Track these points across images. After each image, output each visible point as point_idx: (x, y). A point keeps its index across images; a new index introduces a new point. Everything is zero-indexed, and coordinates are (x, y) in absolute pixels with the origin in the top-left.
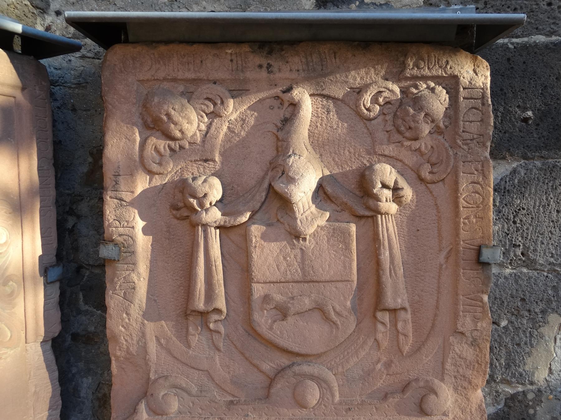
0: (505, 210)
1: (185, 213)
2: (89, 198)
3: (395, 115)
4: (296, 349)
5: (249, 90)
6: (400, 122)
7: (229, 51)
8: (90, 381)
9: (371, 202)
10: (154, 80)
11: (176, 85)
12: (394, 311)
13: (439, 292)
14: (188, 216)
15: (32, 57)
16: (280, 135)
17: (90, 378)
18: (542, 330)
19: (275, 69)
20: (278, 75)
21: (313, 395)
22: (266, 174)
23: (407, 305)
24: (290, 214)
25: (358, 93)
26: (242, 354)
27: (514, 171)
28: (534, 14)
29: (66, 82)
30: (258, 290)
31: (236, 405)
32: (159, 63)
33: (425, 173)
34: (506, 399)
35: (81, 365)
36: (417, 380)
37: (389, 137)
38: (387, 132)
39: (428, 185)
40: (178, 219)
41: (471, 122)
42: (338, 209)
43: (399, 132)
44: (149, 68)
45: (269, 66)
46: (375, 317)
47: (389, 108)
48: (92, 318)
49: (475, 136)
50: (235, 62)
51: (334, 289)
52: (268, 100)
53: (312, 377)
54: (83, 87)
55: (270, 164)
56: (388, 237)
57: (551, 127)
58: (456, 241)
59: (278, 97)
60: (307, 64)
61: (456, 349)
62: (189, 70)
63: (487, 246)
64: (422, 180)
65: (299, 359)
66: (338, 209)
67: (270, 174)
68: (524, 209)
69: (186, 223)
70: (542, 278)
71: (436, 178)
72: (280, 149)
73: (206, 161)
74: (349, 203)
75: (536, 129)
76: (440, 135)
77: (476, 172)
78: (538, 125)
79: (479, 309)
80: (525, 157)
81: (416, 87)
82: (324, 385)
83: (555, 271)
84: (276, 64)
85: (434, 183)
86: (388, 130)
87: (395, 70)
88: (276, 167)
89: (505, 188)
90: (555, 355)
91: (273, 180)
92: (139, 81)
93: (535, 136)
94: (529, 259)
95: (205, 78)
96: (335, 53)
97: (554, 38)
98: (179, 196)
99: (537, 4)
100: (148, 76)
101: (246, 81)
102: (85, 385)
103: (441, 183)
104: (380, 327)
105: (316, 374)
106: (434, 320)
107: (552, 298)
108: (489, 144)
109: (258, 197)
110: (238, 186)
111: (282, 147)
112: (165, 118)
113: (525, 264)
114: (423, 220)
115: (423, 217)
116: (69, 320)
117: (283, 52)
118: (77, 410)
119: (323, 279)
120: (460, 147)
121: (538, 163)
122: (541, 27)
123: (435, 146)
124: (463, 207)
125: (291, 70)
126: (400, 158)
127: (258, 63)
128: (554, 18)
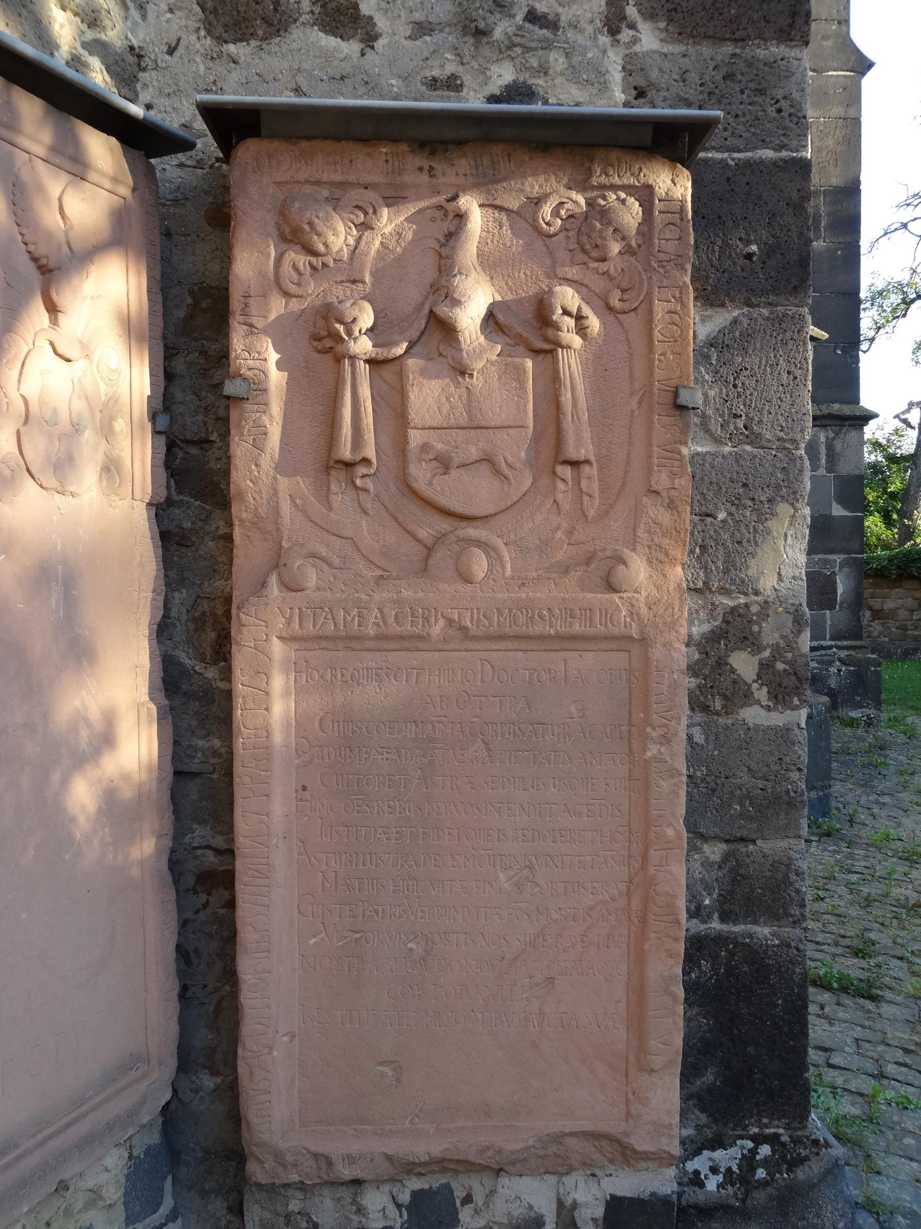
0: (724, 370)
1: (328, 343)
2: (186, 352)
3: (579, 231)
4: (459, 508)
6: (584, 239)
7: (384, 150)
8: (184, 595)
9: (550, 332)
10: (294, 182)
11: (320, 189)
13: (630, 444)
14: (332, 348)
15: (143, 153)
16: (444, 251)
17: (184, 591)
18: (769, 524)
19: (438, 173)
20: (442, 180)
21: (480, 565)
22: (427, 298)
23: (593, 459)
25: (536, 204)
26: (394, 518)
27: (735, 321)
28: (760, 122)
30: (416, 438)
32: (300, 162)
33: (615, 302)
34: (724, 614)
36: (604, 550)
37: (573, 257)
38: (570, 251)
40: (319, 352)
41: (668, 240)
42: (512, 342)
43: (584, 251)
45: (431, 169)
46: (554, 472)
48: (188, 511)
49: (673, 257)
50: (390, 162)
51: (506, 437)
52: (429, 211)
54: (181, 205)
55: (431, 287)
56: (570, 376)
57: (781, 265)
60: (477, 167)
61: (650, 511)
62: (336, 171)
63: (685, 387)
64: (610, 309)
65: (463, 524)
66: (512, 342)
67: (431, 298)
68: (746, 369)
69: (328, 358)
70: (770, 458)
71: (626, 306)
72: (443, 268)
73: (354, 282)
74: (525, 334)
77: (673, 300)
78: (764, 263)
79: (677, 463)
80: (749, 304)
81: (604, 198)
82: (493, 554)
83: (786, 448)
84: (439, 167)
85: (624, 312)
86: (571, 248)
87: (580, 178)
88: (438, 290)
89: (723, 342)
91: (435, 305)
92: (275, 183)
93: (761, 276)
95: (355, 181)
97: (785, 154)
98: (321, 323)
99: (764, 111)
100: (286, 177)
101: (403, 186)
102: (178, 601)
103: (633, 313)
104: (560, 484)
105: (484, 539)
106: (624, 478)
108: (689, 267)
109: (416, 325)
110: (393, 313)
111: (445, 265)
112: (307, 227)
114: (613, 358)
117: (448, 154)
119: (492, 424)
120: (655, 269)
121: (765, 312)
122: (768, 139)
123: (626, 269)
126: (585, 282)
127: (418, 165)
128: (784, 128)
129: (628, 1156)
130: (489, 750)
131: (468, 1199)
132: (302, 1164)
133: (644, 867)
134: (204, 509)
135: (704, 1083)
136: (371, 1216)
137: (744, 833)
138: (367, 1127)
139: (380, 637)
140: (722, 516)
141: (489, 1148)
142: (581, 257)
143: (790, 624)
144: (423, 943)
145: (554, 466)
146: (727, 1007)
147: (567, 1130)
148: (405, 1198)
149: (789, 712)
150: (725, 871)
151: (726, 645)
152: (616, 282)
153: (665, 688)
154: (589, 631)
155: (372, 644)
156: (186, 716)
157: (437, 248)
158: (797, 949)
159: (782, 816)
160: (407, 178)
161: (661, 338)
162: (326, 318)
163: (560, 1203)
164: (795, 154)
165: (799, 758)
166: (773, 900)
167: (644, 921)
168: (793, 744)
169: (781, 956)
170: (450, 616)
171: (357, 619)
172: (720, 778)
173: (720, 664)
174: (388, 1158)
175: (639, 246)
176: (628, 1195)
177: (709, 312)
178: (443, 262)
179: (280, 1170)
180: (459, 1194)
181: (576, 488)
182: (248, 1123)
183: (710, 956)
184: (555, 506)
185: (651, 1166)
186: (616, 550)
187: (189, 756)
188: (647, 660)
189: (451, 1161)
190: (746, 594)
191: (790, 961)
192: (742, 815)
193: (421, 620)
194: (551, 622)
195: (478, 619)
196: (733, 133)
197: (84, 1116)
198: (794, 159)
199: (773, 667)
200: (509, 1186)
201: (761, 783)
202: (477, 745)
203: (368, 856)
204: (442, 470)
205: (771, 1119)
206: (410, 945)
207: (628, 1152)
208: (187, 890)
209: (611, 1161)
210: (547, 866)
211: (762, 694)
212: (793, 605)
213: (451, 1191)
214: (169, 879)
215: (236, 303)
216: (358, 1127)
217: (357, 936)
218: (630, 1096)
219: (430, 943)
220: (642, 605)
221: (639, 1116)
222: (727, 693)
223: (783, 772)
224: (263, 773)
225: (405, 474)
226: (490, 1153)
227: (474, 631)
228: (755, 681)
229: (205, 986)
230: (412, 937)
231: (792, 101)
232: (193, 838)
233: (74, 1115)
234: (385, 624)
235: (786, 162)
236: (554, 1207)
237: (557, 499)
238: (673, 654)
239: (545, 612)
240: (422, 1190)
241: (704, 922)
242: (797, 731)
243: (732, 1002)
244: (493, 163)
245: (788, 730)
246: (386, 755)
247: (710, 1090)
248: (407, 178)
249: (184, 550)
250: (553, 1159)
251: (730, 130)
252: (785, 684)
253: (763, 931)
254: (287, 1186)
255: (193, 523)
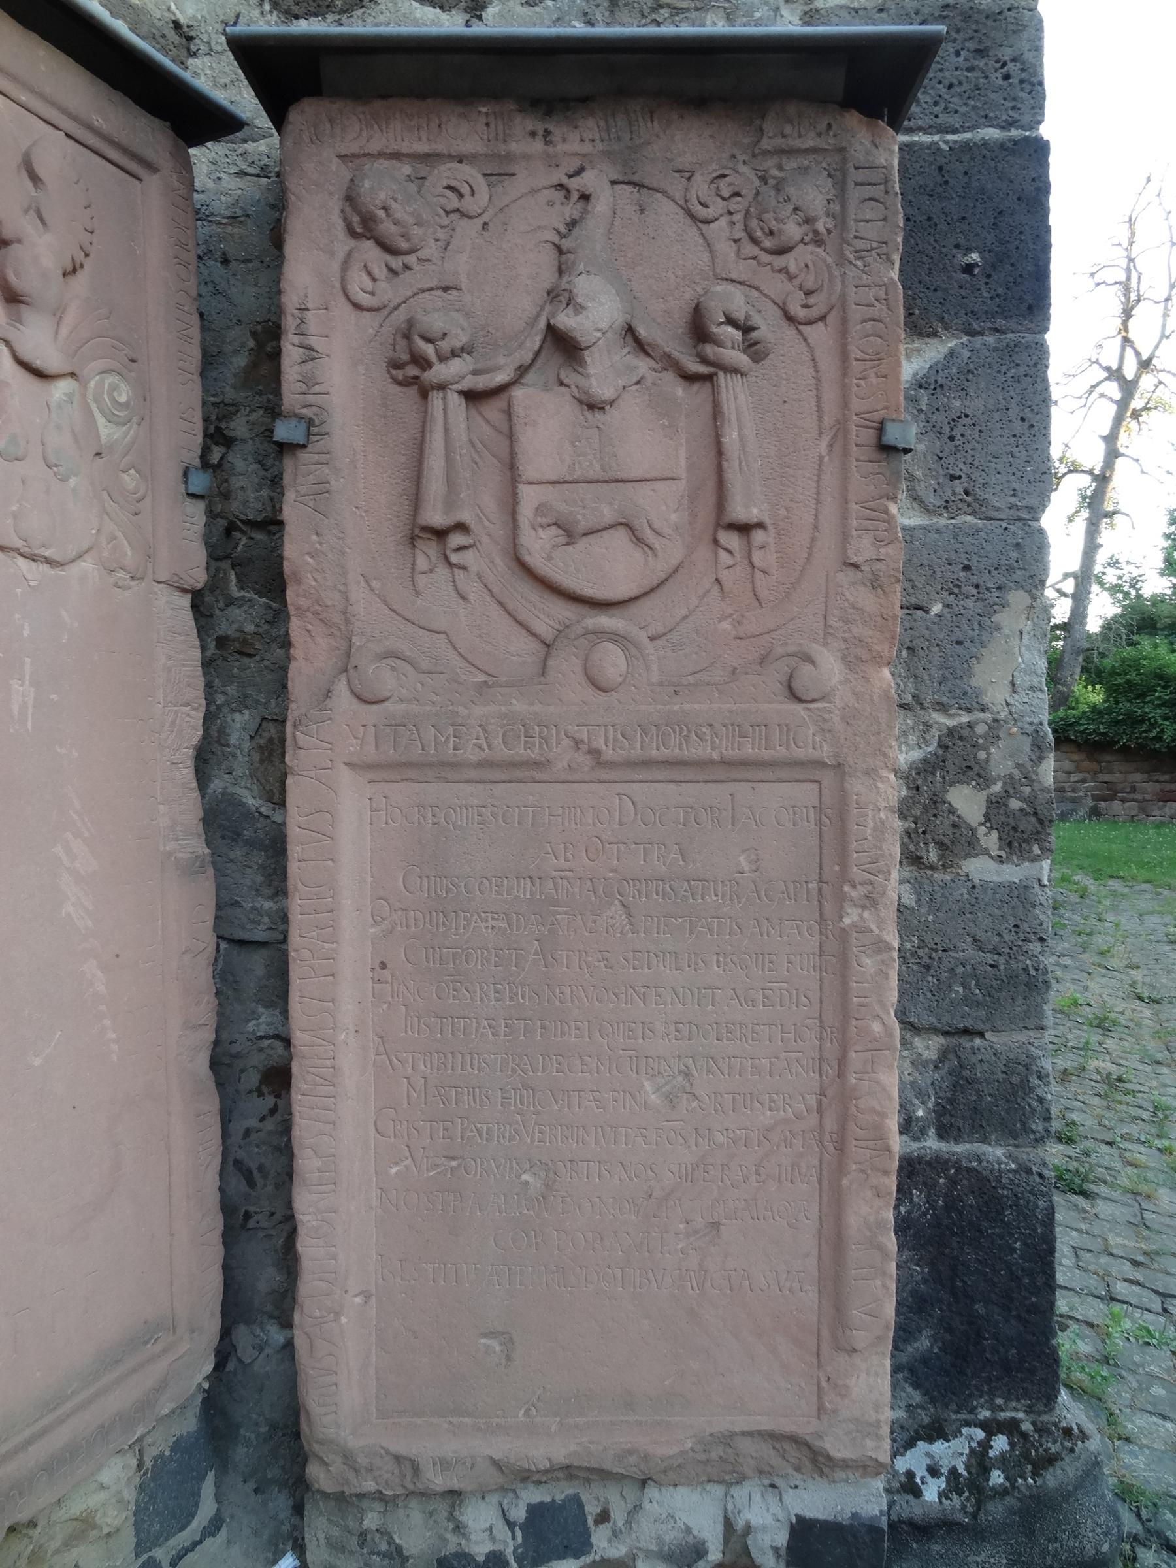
0: (938, 418)
1: (412, 371)
3: (747, 212)
4: (588, 591)
5: (513, 175)
6: (754, 223)
7: (484, 110)
8: (246, 717)
9: (709, 350)
10: (365, 155)
11: (399, 164)
12: (744, 529)
13: (818, 502)
14: (417, 378)
15: (168, 124)
16: (565, 244)
17: (246, 712)
19: (557, 136)
20: (561, 148)
23: (768, 521)
24: (580, 370)
25: (689, 179)
26: (501, 604)
27: (952, 353)
29: (212, 214)
30: (529, 497)
31: (490, 687)
32: (372, 127)
35: (231, 690)
37: (739, 250)
38: (735, 241)
39: (800, 327)
40: (400, 383)
43: (754, 241)
44: (356, 135)
45: (547, 133)
46: (716, 541)
47: (738, 203)
48: (251, 611)
49: (875, 245)
50: (492, 126)
52: (545, 192)
53: (615, 637)
54: (241, 222)
55: (549, 293)
56: (737, 409)
57: (1011, 279)
58: (844, 415)
59: (561, 185)
60: (608, 131)
61: (847, 593)
62: (420, 139)
63: (893, 420)
64: (790, 318)
66: (657, 366)
67: (548, 308)
68: (967, 416)
69: (413, 391)
71: (815, 313)
72: (563, 267)
73: (446, 289)
74: (675, 354)
75: (987, 283)
76: (819, 246)
77: (876, 303)
78: (989, 276)
79: (883, 525)
80: (971, 333)
81: (780, 168)
82: (634, 651)
83: (1020, 519)
84: (557, 131)
86: (736, 238)
87: (747, 141)
88: (558, 296)
89: (936, 381)
90: (1020, 660)
91: (553, 316)
92: (340, 157)
93: (985, 294)
94: (976, 500)
95: (445, 152)
96: (652, 113)
98: (402, 343)
100: (354, 148)
101: (509, 157)
102: (238, 725)
103: (820, 324)
104: (723, 555)
106: (811, 548)
107: (1015, 564)
108: (897, 258)
109: (528, 344)
113: (970, 510)
114: (793, 386)
115: (793, 379)
116: (211, 616)
118: (223, 767)
120: (850, 262)
121: (990, 339)
123: (810, 264)
124: (856, 360)
125: (582, 140)
127: (530, 127)
129: (820, 1463)
130: (629, 915)
131: (604, 1517)
132: (380, 1469)
133: (841, 1074)
134: (270, 607)
135: (917, 1350)
136: (473, 1537)
137: (969, 1023)
138: (467, 1419)
139: (482, 764)
140: (937, 608)
141: (630, 1452)
142: (749, 249)
143: (1027, 748)
144: (542, 1174)
145: (715, 532)
146: (947, 1251)
147: (737, 1430)
148: (519, 1513)
149: (1027, 864)
150: (943, 1072)
151: (944, 778)
152: (797, 282)
153: (869, 831)
154: (767, 754)
155: (472, 774)
156: (248, 871)
157: (556, 239)
158: (1041, 1176)
159: (1020, 1000)
160: (514, 147)
161: (860, 355)
162: (407, 337)
163: (728, 1524)
164: (1027, 133)
165: (1041, 925)
166: (1008, 1111)
167: (841, 1146)
168: (1034, 906)
169: (1018, 1185)
170: (577, 735)
171: (452, 739)
172: (936, 951)
173: (935, 802)
174: (496, 1464)
175: (829, 232)
176: (821, 1516)
177: (916, 345)
178: (564, 258)
179: (351, 1475)
180: (592, 1509)
181: (746, 562)
182: (307, 1412)
183: (925, 1184)
184: (717, 587)
185: (851, 1476)
186: (800, 644)
187: (253, 921)
188: (843, 793)
189: (579, 1468)
190: (969, 710)
191: (1031, 1192)
192: (965, 1000)
193: (537, 740)
194: (713, 742)
195: (615, 739)
196: (946, 108)
197: (61, 1421)
198: (1027, 138)
199: (1006, 805)
200: (657, 1501)
201: (990, 958)
202: (613, 909)
203: (468, 1058)
204: (563, 540)
205: (1008, 1399)
206: (525, 1177)
207: (821, 1459)
208: (250, 1092)
209: (798, 1469)
210: (708, 1071)
211: (991, 841)
212: (1031, 723)
213: (581, 1505)
214: (210, 1083)
215: (289, 318)
216: (455, 1420)
217: (454, 1163)
218: (824, 1384)
219: (551, 1175)
220: (836, 719)
221: (834, 1411)
222: (946, 840)
223: (1020, 943)
224: (327, 946)
225: (515, 545)
226: (632, 1460)
227: (608, 753)
228: (983, 824)
229: (273, 1214)
230: (527, 1166)
231: (1023, 63)
232: (258, 1025)
233: (46, 1421)
234: (489, 747)
235: (1016, 143)
236: (720, 1528)
237: (720, 576)
238: (880, 785)
239: (704, 730)
240: (541, 1504)
241: (916, 1139)
242: (1037, 889)
243: (954, 1244)
244: (630, 124)
245: (1026, 887)
246: (491, 923)
247: (925, 1360)
248: (514, 147)
249: (246, 660)
250: (720, 1464)
251: (942, 105)
252: (1021, 828)
253: (995, 1153)
254: (361, 1496)
255: (257, 626)
